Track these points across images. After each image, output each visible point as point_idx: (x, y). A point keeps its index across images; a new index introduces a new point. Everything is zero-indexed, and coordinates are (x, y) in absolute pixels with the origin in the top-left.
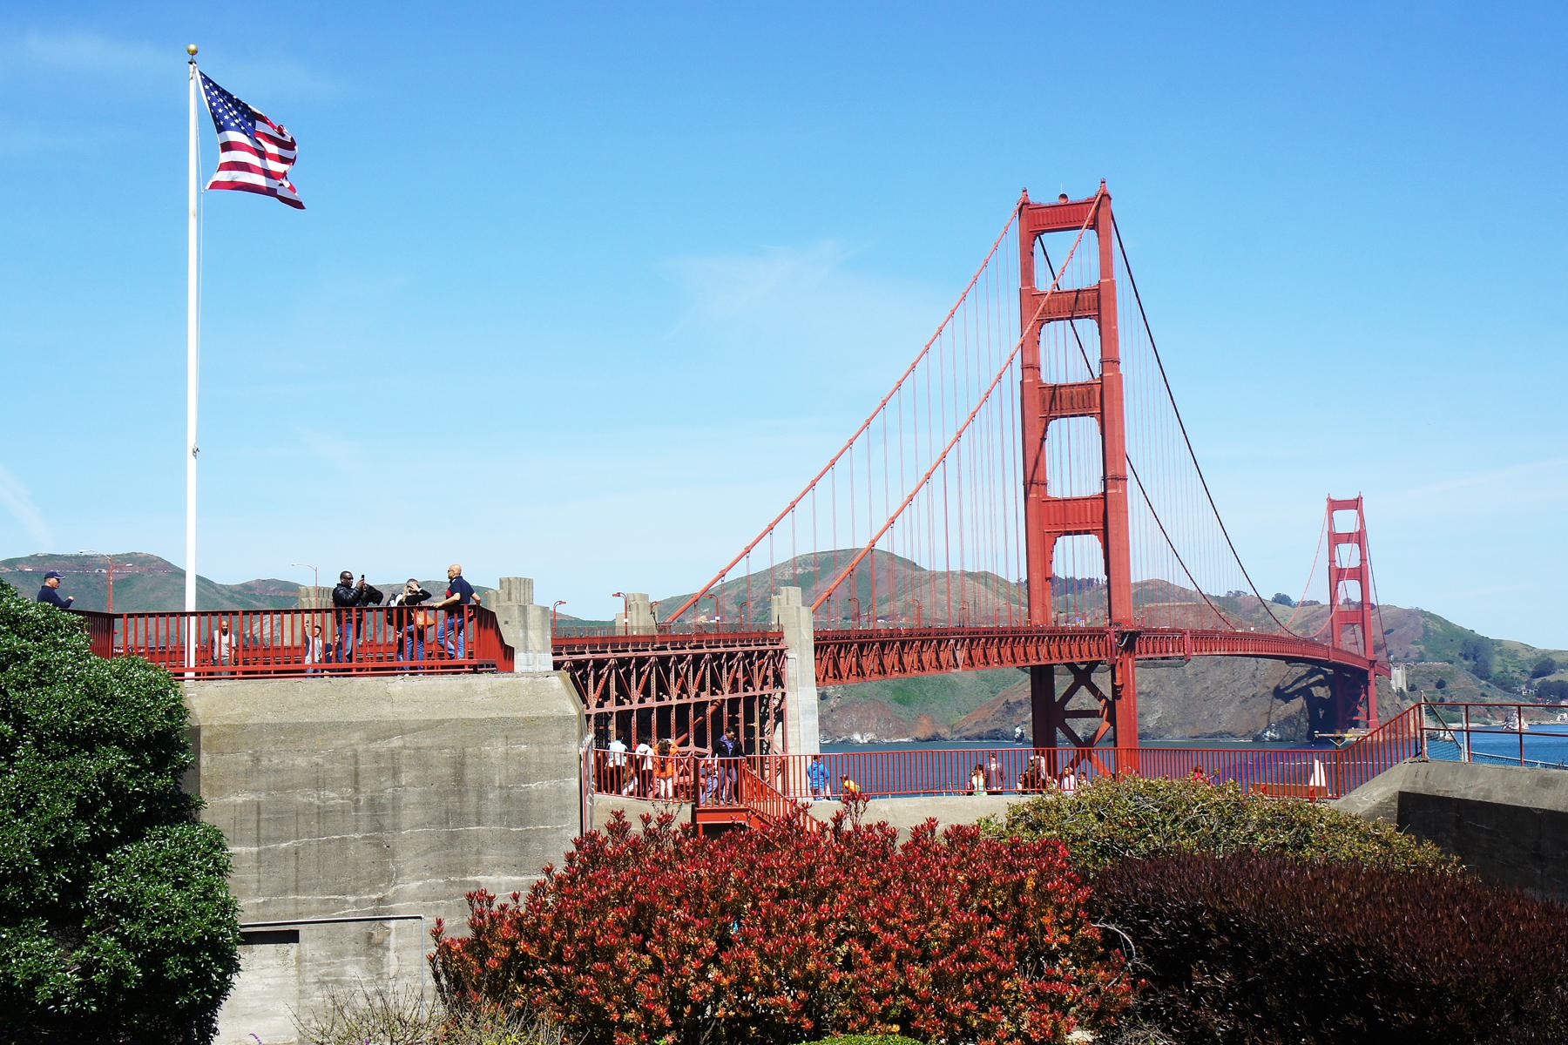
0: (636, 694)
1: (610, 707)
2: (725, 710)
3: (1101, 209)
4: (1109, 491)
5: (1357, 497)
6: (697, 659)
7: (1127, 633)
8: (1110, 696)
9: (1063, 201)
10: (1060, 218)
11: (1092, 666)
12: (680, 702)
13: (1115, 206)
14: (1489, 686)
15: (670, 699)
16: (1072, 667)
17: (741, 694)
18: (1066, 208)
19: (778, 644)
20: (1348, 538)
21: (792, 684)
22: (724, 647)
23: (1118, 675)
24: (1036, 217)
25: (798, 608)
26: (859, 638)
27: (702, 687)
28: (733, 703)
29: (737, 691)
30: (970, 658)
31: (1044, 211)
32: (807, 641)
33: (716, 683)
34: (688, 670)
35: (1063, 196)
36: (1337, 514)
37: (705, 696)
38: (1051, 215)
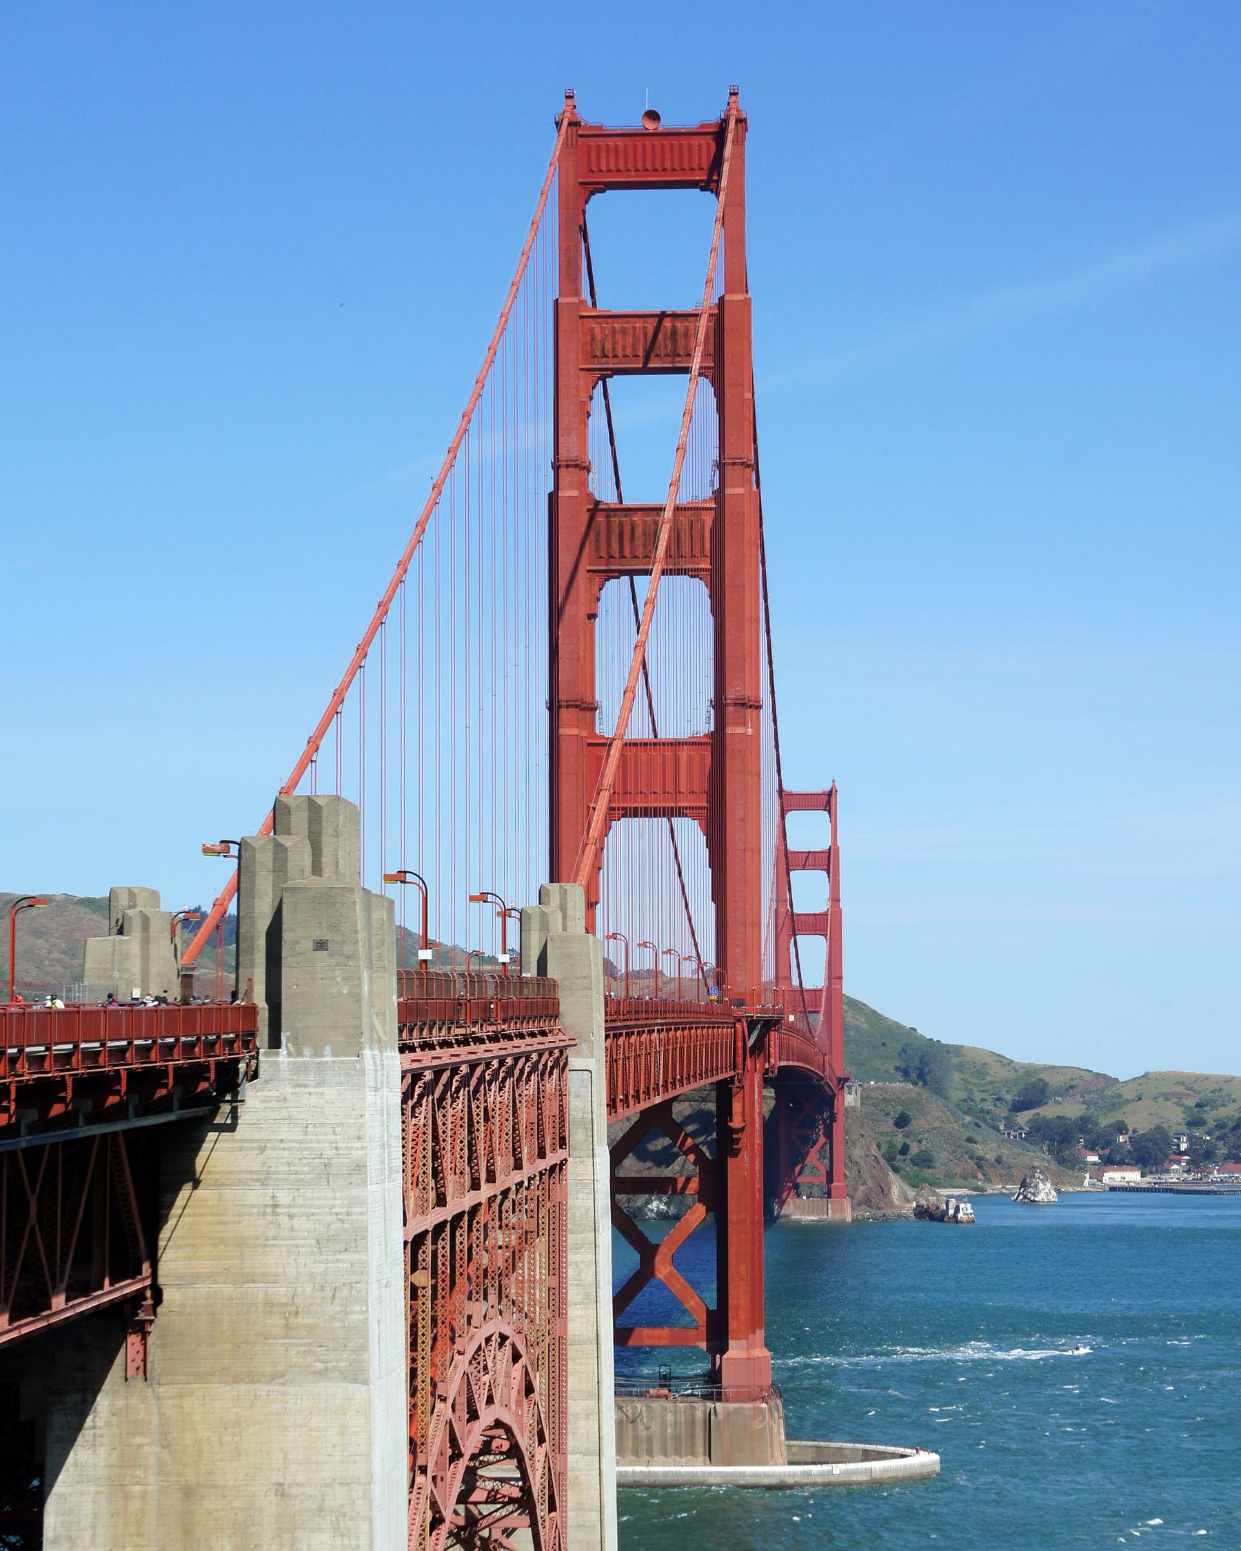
4: (729, 730)
5: (827, 788)
7: (757, 1021)
9: (650, 126)
10: (644, 161)
18: (656, 141)
20: (809, 860)
23: (737, 1107)
24: (594, 155)
31: (611, 142)
35: (652, 115)
38: (626, 152)
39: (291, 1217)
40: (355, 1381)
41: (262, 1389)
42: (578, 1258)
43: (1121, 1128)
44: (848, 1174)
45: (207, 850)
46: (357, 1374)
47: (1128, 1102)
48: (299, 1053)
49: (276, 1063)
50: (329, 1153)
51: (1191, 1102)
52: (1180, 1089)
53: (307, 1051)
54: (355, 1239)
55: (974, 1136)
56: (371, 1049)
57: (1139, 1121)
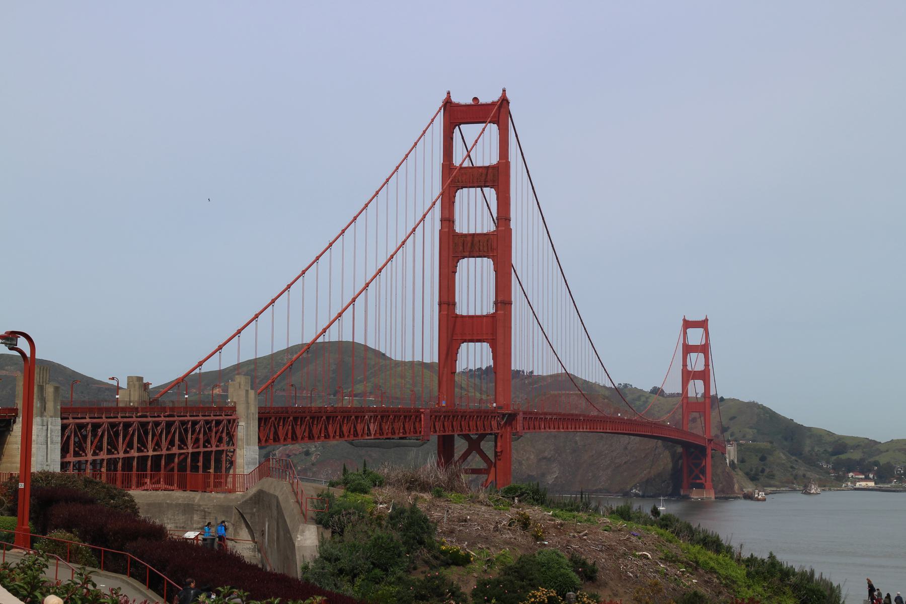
0: (121, 447)
1: (103, 455)
2: (189, 460)
3: (502, 110)
5: (704, 318)
6: (169, 425)
7: (506, 414)
8: (492, 459)
11: (482, 437)
12: (155, 453)
13: (512, 107)
14: (796, 461)
15: (148, 451)
16: (467, 437)
17: (202, 449)
19: (231, 415)
21: (240, 443)
22: (191, 416)
23: (499, 444)
25: (247, 391)
26: (295, 412)
27: (172, 443)
28: (195, 456)
29: (198, 447)
30: (381, 429)
32: (253, 414)
33: (183, 442)
34: (162, 432)
36: (689, 331)
37: (175, 450)
43: (876, 463)
44: (714, 479)
47: (882, 452)
57: (883, 459)
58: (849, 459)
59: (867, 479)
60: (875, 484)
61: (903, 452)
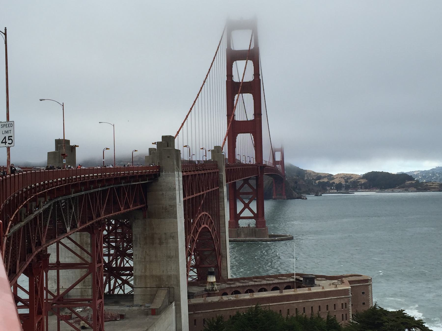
39: (165, 196)
40: (175, 218)
41: (162, 220)
42: (221, 203)
43: (334, 183)
45: (153, 143)
46: (176, 218)
47: (335, 179)
48: (166, 173)
49: (163, 174)
50: (170, 186)
51: (346, 178)
52: (344, 176)
53: (167, 172)
54: (175, 199)
55: (308, 185)
56: (176, 172)
57: (337, 181)
58: (323, 181)
59: (331, 189)
60: (337, 191)
61: (343, 178)
